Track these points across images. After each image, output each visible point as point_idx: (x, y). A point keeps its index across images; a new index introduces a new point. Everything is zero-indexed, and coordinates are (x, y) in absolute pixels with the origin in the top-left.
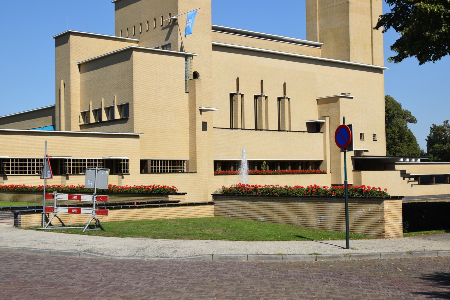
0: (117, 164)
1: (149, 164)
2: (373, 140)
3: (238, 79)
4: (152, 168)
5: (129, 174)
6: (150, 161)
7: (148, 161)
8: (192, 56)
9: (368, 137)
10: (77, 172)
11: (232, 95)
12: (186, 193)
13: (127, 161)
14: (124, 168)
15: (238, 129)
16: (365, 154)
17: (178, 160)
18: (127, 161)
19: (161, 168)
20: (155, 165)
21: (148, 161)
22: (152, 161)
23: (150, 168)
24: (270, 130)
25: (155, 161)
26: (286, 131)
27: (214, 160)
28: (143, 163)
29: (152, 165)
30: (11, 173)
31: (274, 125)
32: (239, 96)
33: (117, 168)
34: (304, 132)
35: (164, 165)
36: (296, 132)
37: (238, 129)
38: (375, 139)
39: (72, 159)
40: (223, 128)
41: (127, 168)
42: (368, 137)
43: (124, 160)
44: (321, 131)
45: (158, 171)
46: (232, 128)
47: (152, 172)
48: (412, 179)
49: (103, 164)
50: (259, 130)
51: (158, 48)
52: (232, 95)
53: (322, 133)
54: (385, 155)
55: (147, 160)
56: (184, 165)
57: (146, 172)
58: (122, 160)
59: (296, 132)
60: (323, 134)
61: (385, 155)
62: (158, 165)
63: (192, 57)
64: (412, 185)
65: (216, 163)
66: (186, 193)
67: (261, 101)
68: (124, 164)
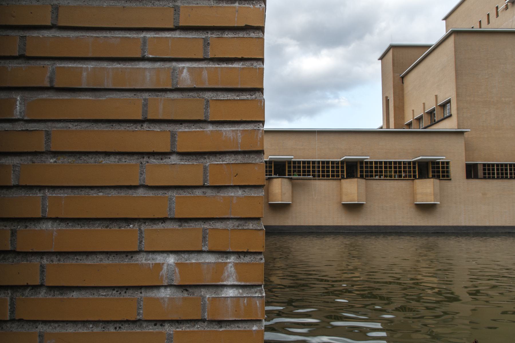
4: (485, 174)
5: (450, 179)
7: (479, 166)
10: (372, 176)
13: (448, 163)
14: (443, 172)
18: (448, 163)
20: (489, 170)
21: (478, 164)
22: (484, 165)
23: (482, 174)
25: (489, 165)
29: (484, 170)
30: (332, 177)
41: (448, 172)
43: (443, 163)
47: (485, 178)
55: (477, 164)
57: (476, 177)
58: (440, 162)
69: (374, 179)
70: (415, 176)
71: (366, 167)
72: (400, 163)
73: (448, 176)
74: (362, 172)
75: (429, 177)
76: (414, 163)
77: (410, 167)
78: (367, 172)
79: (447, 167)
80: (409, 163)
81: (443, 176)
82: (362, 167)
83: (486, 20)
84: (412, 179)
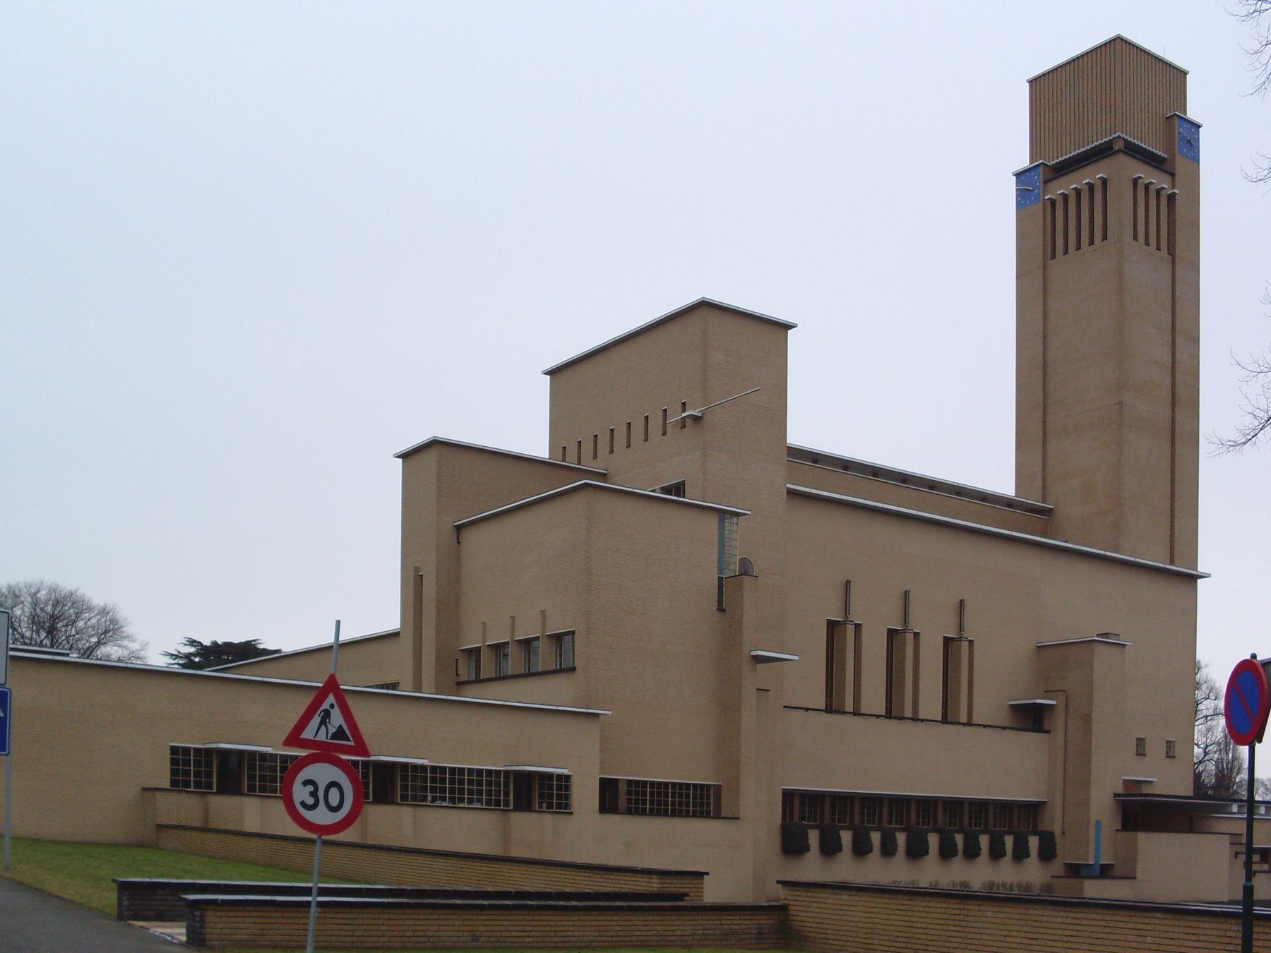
0: (542, 787)
1: (623, 788)
2: (1167, 757)
3: (848, 583)
4: (629, 801)
6: (626, 783)
9: (1155, 750)
11: (832, 625)
12: (707, 874)
14: (559, 797)
16: (1146, 790)
18: (568, 778)
19: (652, 802)
20: (637, 793)
22: (630, 782)
24: (922, 720)
26: (961, 723)
27: (783, 789)
28: (608, 790)
29: (629, 793)
31: (931, 705)
32: (850, 630)
33: (541, 796)
34: (1004, 728)
35: (659, 794)
36: (985, 726)
37: (845, 713)
38: (1171, 754)
39: (432, 767)
40: (807, 709)
41: (567, 797)
42: (1155, 750)
43: (560, 777)
44: (1046, 727)
46: (829, 709)
47: (629, 812)
49: (507, 785)
50: (895, 718)
51: (654, 491)
52: (832, 625)
53: (1048, 732)
54: (1191, 794)
56: (708, 796)
59: (985, 726)
60: (1047, 735)
61: (1191, 794)
62: (644, 794)
65: (788, 796)
66: (707, 874)
67: (903, 643)
68: (559, 788)
69: (430, 806)
70: (507, 804)
71: (414, 779)
72: (480, 772)
73: (567, 806)
74: (405, 788)
75: (533, 808)
76: (507, 773)
77: (498, 784)
78: (414, 788)
79: (567, 788)
80: (498, 772)
81: (559, 806)
83: (642, 430)
84: (503, 810)
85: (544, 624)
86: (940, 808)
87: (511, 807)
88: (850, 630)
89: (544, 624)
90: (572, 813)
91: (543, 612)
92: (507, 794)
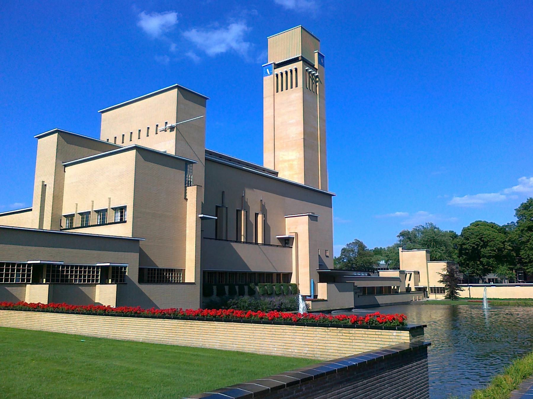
0: (113, 273)
1: (146, 272)
4: (148, 277)
8: (192, 163)
11: (217, 207)
13: (125, 268)
14: (121, 276)
15: (223, 240)
17: (167, 269)
22: (149, 269)
29: (149, 273)
32: (224, 209)
37: (223, 240)
43: (121, 267)
45: (154, 281)
48: (359, 291)
52: (217, 207)
55: (144, 268)
63: (191, 165)
64: (359, 296)
82: (48, 271)
85: (110, 203)
86: (257, 275)
87: (99, 282)
88: (224, 209)
89: (110, 203)
90: (126, 284)
91: (110, 198)
92: (97, 276)
